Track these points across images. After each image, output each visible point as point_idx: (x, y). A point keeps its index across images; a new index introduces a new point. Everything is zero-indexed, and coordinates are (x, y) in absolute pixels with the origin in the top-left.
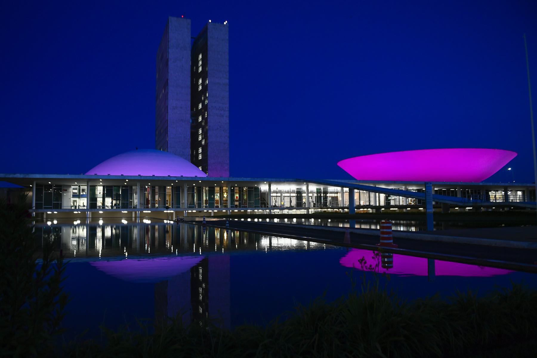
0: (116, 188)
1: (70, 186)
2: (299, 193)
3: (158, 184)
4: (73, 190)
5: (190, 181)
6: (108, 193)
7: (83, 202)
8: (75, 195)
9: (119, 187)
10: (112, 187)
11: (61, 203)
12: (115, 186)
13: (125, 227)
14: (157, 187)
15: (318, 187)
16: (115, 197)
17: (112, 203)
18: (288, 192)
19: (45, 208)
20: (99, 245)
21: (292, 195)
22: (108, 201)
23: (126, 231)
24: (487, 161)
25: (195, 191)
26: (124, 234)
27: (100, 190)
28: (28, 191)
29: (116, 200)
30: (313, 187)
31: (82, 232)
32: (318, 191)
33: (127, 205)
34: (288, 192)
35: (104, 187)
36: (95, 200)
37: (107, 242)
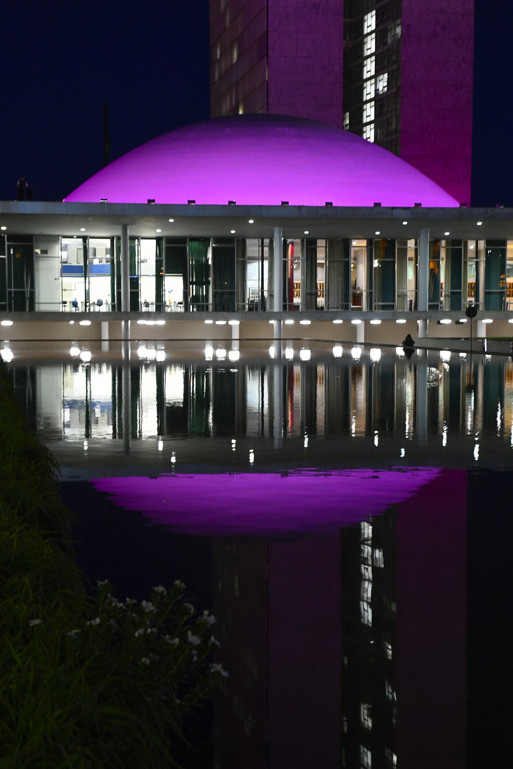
1: (55, 239)
4: (68, 249)
7: (101, 289)
8: (67, 270)
9: (205, 241)
11: (32, 294)
12: (193, 239)
13: (223, 369)
14: (321, 243)
16: (195, 276)
17: (186, 294)
20: (149, 424)
22: (174, 285)
23: (227, 384)
25: (443, 254)
26: (218, 393)
27: (147, 251)
29: (199, 284)
31: (102, 386)
33: (228, 300)
35: (159, 240)
37: (172, 419)
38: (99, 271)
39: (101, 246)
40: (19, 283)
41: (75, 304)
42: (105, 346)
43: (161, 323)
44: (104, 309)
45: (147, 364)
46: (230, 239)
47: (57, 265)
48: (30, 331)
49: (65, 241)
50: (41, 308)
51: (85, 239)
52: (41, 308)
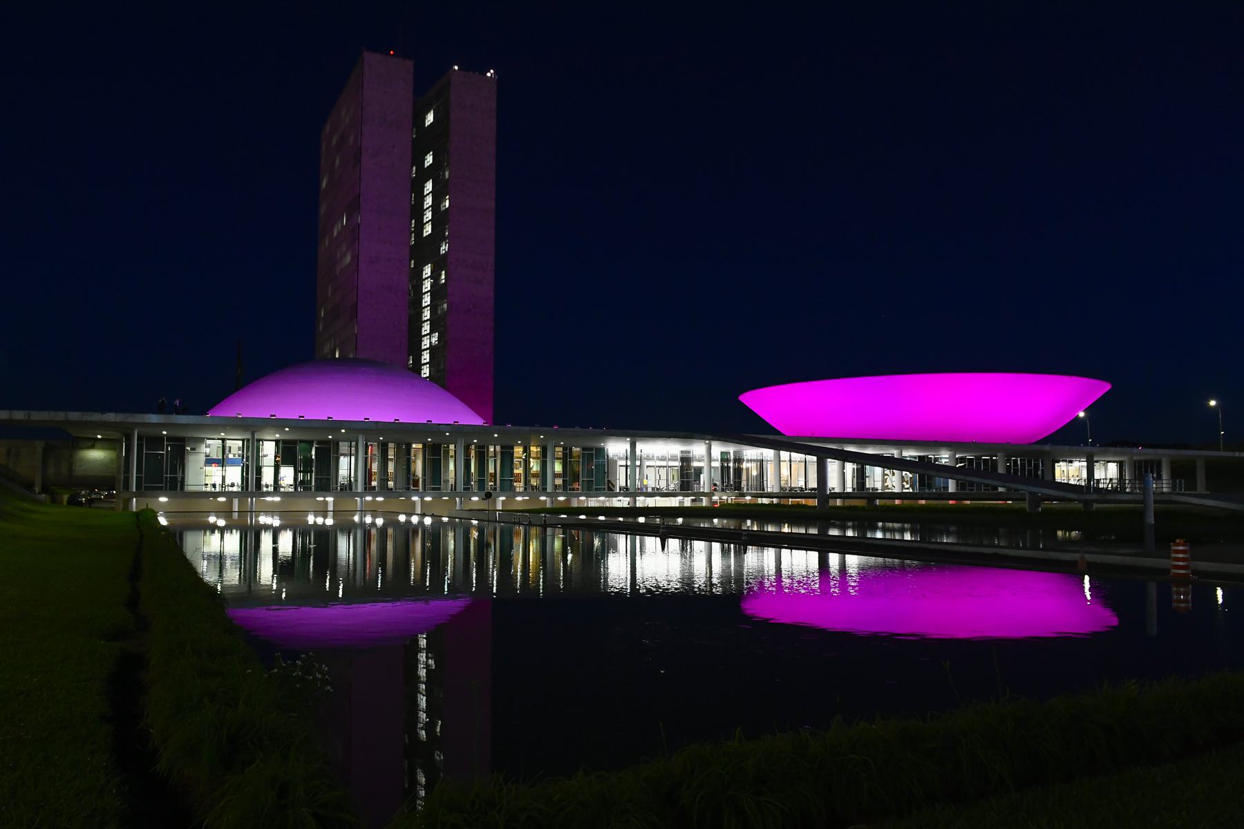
0: (303, 445)
1: (202, 440)
2: (686, 460)
3: (396, 437)
4: (212, 447)
5: (459, 432)
6: (286, 454)
7: (234, 475)
8: (210, 461)
9: (310, 443)
10: (294, 442)
11: (183, 479)
12: (301, 441)
14: (391, 445)
15: (724, 449)
16: (302, 466)
17: (295, 479)
18: (663, 459)
19: (147, 488)
20: (266, 571)
21: (671, 463)
24: (1068, 397)
25: (473, 454)
26: (318, 546)
27: (269, 449)
28: (88, 448)
29: (305, 472)
30: (717, 449)
31: (232, 543)
32: (724, 458)
33: (326, 482)
34: (663, 459)
35: (277, 442)
36: (259, 471)
37: (282, 568)
38: (233, 463)
39: (235, 445)
40: (174, 471)
41: (214, 486)
42: (235, 515)
43: (277, 499)
44: (235, 489)
45: (267, 527)
46: (329, 442)
47: (203, 458)
48: (180, 505)
49: (209, 442)
50: (190, 488)
51: (223, 440)
52: (190, 488)
